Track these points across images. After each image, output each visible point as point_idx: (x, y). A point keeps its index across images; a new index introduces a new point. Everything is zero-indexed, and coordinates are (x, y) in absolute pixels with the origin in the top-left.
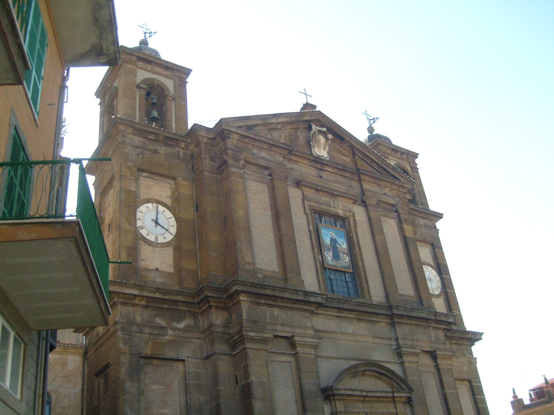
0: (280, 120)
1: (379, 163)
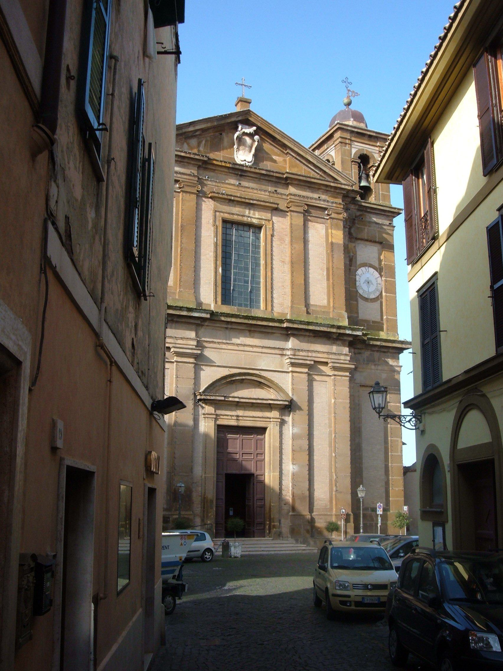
0: (198, 127)
1: (315, 162)
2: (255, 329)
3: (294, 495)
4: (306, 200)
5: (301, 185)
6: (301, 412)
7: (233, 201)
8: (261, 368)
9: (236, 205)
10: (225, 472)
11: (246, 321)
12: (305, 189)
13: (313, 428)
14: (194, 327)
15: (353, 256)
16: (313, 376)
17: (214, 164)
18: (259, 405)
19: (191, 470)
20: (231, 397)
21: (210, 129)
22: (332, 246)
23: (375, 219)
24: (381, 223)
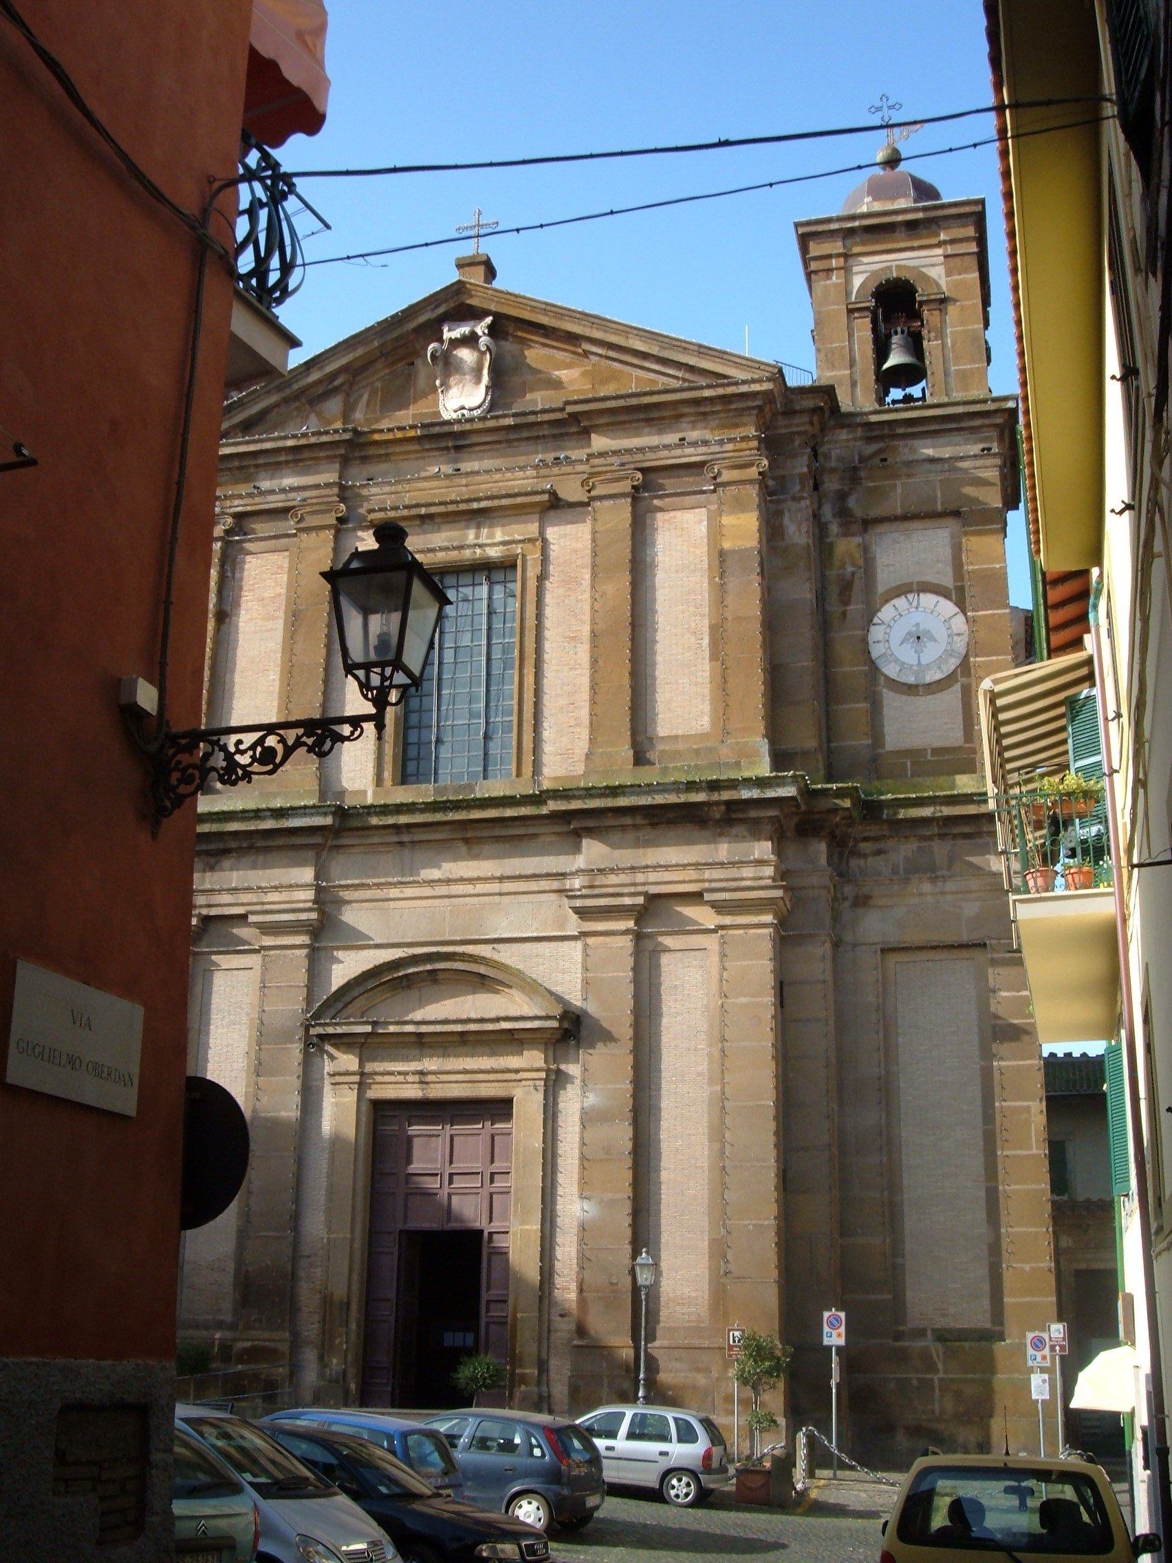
0: (331, 368)
2: (478, 834)
3: (584, 1287)
4: (639, 457)
5: (625, 422)
6: (611, 1045)
7: (430, 517)
8: (496, 936)
9: (444, 527)
10: (400, 1226)
11: (439, 817)
12: (637, 428)
13: (659, 1089)
14: (311, 854)
15: (853, 574)
16: (660, 939)
17: (376, 443)
18: (479, 1037)
19: (295, 1219)
20: (392, 1023)
21: (372, 362)
22: (722, 560)
23: (930, 452)
24: (947, 456)
